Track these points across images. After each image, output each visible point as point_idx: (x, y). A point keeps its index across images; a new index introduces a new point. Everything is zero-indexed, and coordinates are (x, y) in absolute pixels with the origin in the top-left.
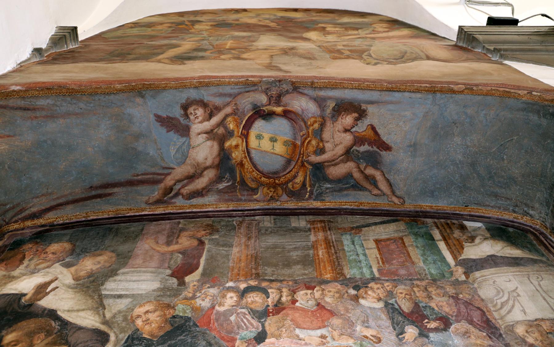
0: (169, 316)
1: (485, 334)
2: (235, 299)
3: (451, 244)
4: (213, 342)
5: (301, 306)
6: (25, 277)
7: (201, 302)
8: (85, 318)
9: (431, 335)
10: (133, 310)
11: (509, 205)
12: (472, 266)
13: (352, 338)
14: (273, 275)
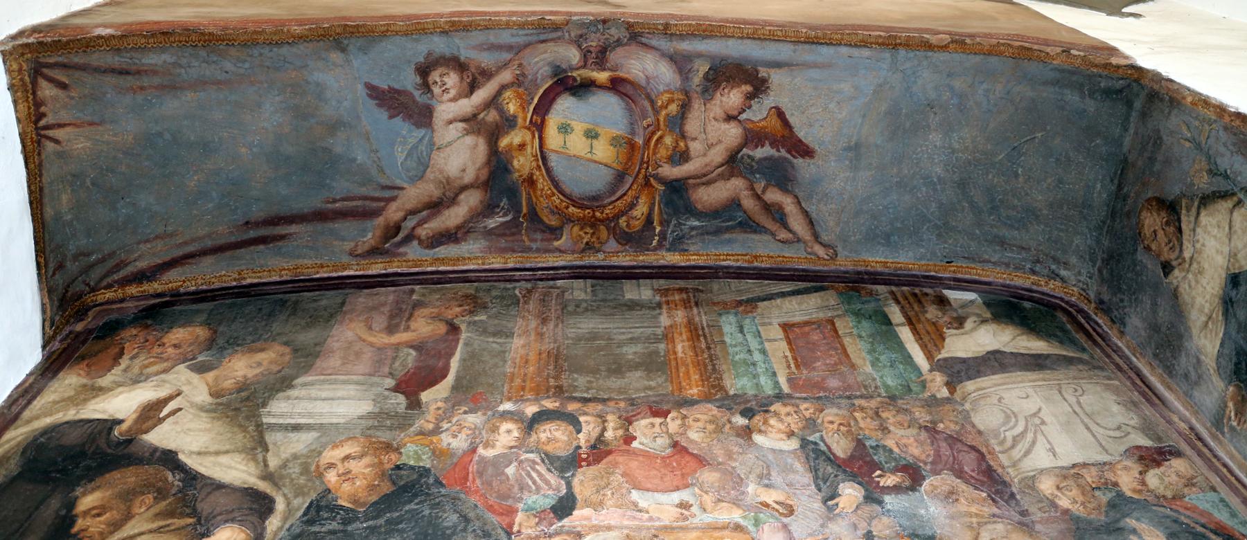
0: (388, 466)
1: (984, 495)
2: (516, 434)
3: (922, 332)
4: (471, 515)
5: (641, 447)
6: (121, 389)
7: (451, 440)
8: (230, 467)
9: (887, 499)
10: (320, 453)
11: (1024, 260)
12: (960, 371)
13: (738, 506)
14: (588, 389)
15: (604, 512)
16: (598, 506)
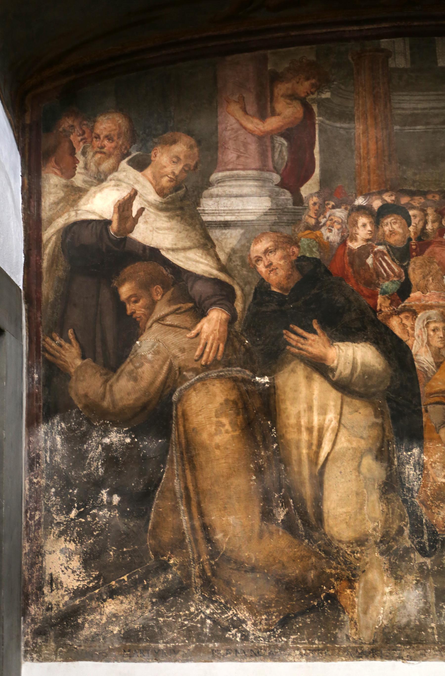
0: (294, 258)
2: (369, 228)
4: (352, 298)
7: (329, 234)
8: (198, 262)
10: (249, 248)
15: (428, 294)
16: (424, 289)
